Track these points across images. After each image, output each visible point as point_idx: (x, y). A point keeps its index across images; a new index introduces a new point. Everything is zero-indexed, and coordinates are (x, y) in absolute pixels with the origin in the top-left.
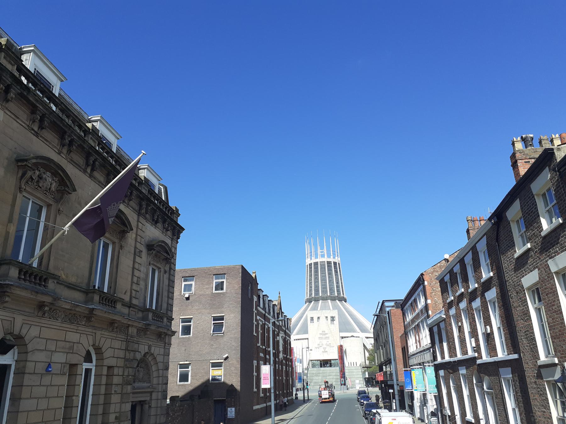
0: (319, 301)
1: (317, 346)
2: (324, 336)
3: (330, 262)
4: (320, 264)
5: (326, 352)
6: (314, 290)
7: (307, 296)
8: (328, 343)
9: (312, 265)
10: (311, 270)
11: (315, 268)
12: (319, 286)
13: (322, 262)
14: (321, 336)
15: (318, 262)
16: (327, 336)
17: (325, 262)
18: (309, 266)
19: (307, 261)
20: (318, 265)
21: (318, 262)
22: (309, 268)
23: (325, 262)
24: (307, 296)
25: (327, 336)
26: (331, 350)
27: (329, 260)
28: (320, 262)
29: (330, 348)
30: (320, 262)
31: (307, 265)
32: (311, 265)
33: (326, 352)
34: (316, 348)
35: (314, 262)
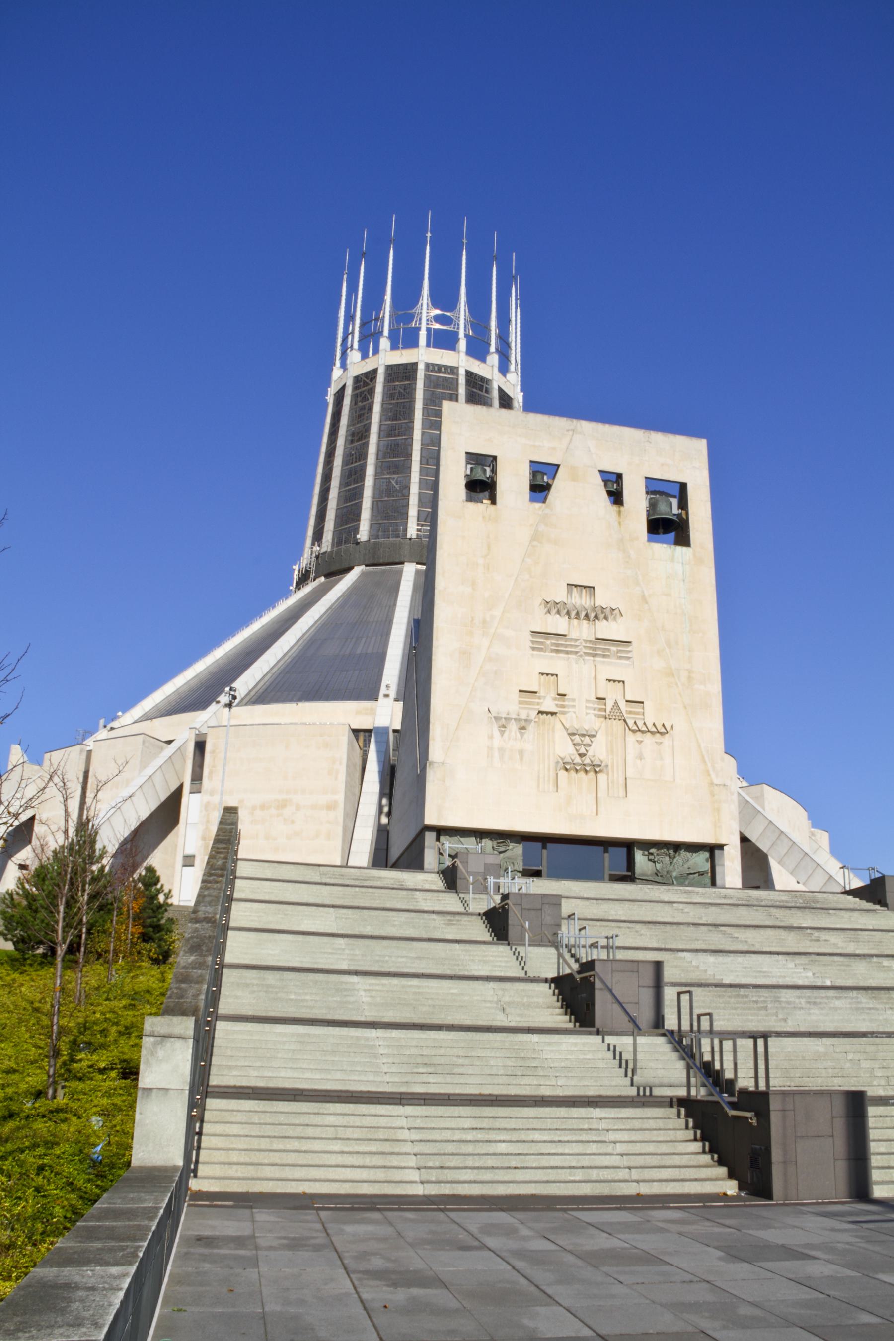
0: (403, 563)
1: (511, 705)
2: (582, 631)
3: (482, 379)
4: (427, 378)
5: (596, 769)
6: (373, 509)
7: (318, 536)
8: (613, 694)
9: (375, 378)
10: (363, 408)
11: (389, 395)
12: (407, 487)
13: (439, 368)
14: (559, 624)
15: (416, 364)
16: (606, 629)
17: (453, 370)
18: (355, 388)
19: (337, 372)
20: (414, 378)
21: (416, 364)
22: (355, 398)
23: (458, 375)
24: (318, 536)
25: (605, 629)
26: (640, 757)
27: (478, 368)
28: (427, 365)
29: (631, 738)
30: (427, 365)
31: (340, 396)
32: (364, 382)
33: (596, 769)
34: (502, 722)
35: (390, 363)
